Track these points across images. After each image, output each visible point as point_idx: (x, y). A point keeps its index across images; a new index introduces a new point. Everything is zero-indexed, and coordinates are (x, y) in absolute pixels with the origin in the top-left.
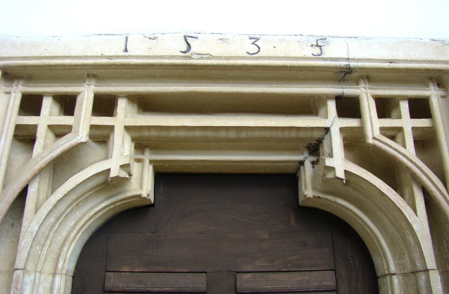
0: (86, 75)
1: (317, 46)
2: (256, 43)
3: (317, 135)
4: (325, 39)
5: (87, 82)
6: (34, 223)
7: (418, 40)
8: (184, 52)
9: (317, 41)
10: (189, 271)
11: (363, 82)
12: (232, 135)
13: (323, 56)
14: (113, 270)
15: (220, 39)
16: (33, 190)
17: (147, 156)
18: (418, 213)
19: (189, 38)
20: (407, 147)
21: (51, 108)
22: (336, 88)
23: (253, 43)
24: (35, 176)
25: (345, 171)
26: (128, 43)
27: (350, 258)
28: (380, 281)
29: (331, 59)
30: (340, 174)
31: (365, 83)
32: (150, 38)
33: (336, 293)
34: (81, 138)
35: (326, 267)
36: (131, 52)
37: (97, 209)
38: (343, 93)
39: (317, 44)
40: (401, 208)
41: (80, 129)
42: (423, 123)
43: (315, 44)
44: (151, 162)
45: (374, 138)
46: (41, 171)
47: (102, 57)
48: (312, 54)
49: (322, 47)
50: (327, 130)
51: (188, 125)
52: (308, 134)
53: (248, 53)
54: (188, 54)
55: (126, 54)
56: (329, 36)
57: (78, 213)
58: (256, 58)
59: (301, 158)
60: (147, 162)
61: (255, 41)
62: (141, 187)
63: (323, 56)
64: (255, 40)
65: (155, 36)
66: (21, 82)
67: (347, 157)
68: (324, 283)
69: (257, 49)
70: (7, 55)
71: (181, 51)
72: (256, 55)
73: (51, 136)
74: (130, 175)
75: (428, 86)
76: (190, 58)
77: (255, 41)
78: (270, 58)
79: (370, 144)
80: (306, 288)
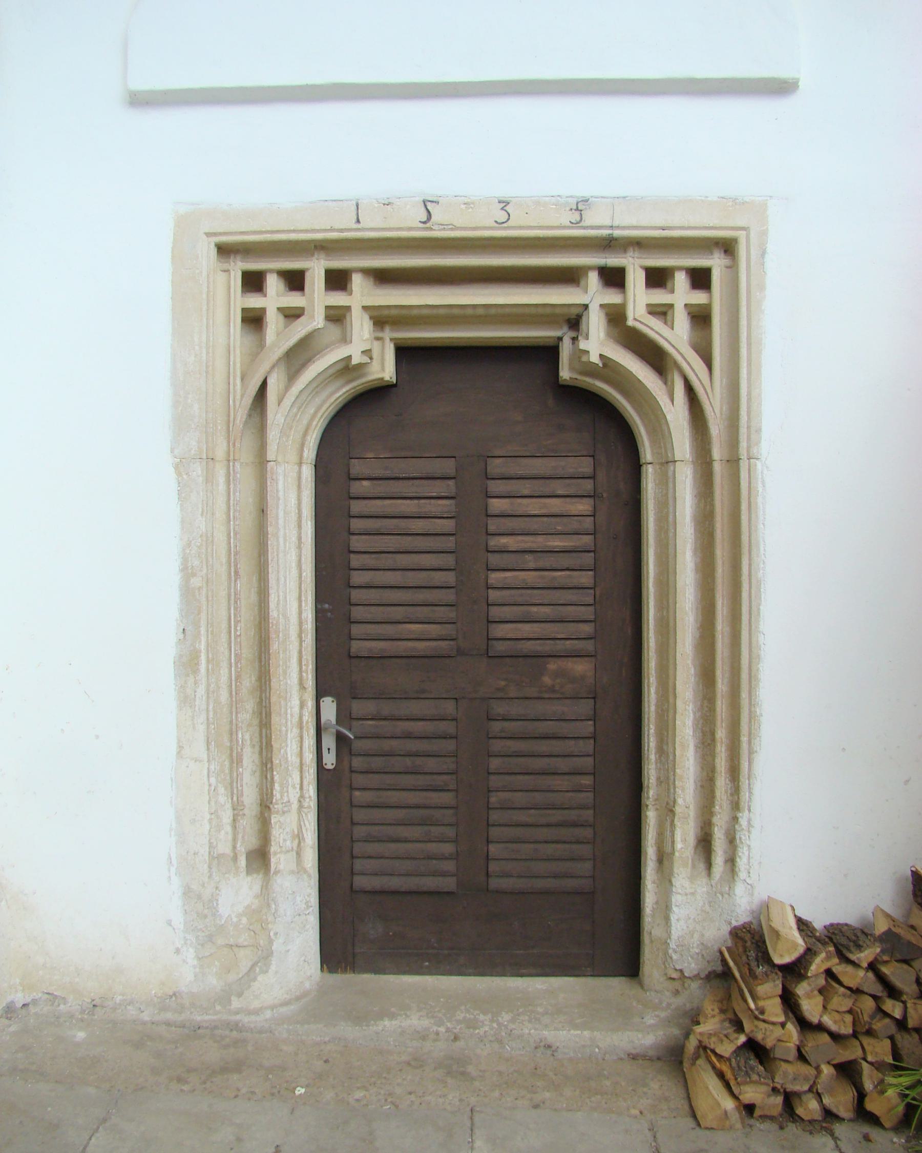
0: (313, 247)
1: (577, 209)
2: (505, 208)
3: (574, 311)
4: (587, 201)
5: (316, 256)
6: (279, 415)
7: (703, 198)
8: (424, 223)
9: (577, 204)
10: (438, 456)
11: (631, 249)
12: (481, 311)
14: (358, 456)
15: (465, 204)
16: (273, 381)
17: (388, 334)
19: (429, 203)
21: (277, 286)
22: (599, 258)
23: (502, 209)
24: (273, 367)
25: (601, 355)
26: (360, 211)
27: (612, 444)
28: (644, 468)
29: (592, 228)
30: (594, 358)
31: (634, 251)
32: (384, 204)
34: (318, 324)
35: (585, 453)
36: (366, 222)
37: (338, 395)
38: (606, 265)
39: (577, 207)
40: (656, 397)
41: (316, 313)
42: (699, 298)
43: (575, 207)
44: (391, 340)
45: (635, 319)
46: (280, 359)
47: (332, 230)
48: (570, 222)
49: (582, 212)
50: (586, 307)
51: (431, 304)
52: (565, 310)
53: (496, 222)
54: (428, 225)
55: (359, 226)
56: (592, 197)
57: (317, 399)
58: (505, 228)
59: (558, 333)
60: (387, 340)
61: (505, 206)
62: (383, 369)
64: (505, 204)
65: (390, 201)
66: (239, 257)
67: (609, 335)
68: (580, 470)
69: (507, 216)
70: (221, 230)
71: (420, 222)
72: (505, 225)
73: (281, 318)
74: (371, 358)
75: (712, 254)
76: (431, 229)
77: (505, 206)
78: (521, 228)
79: (630, 327)
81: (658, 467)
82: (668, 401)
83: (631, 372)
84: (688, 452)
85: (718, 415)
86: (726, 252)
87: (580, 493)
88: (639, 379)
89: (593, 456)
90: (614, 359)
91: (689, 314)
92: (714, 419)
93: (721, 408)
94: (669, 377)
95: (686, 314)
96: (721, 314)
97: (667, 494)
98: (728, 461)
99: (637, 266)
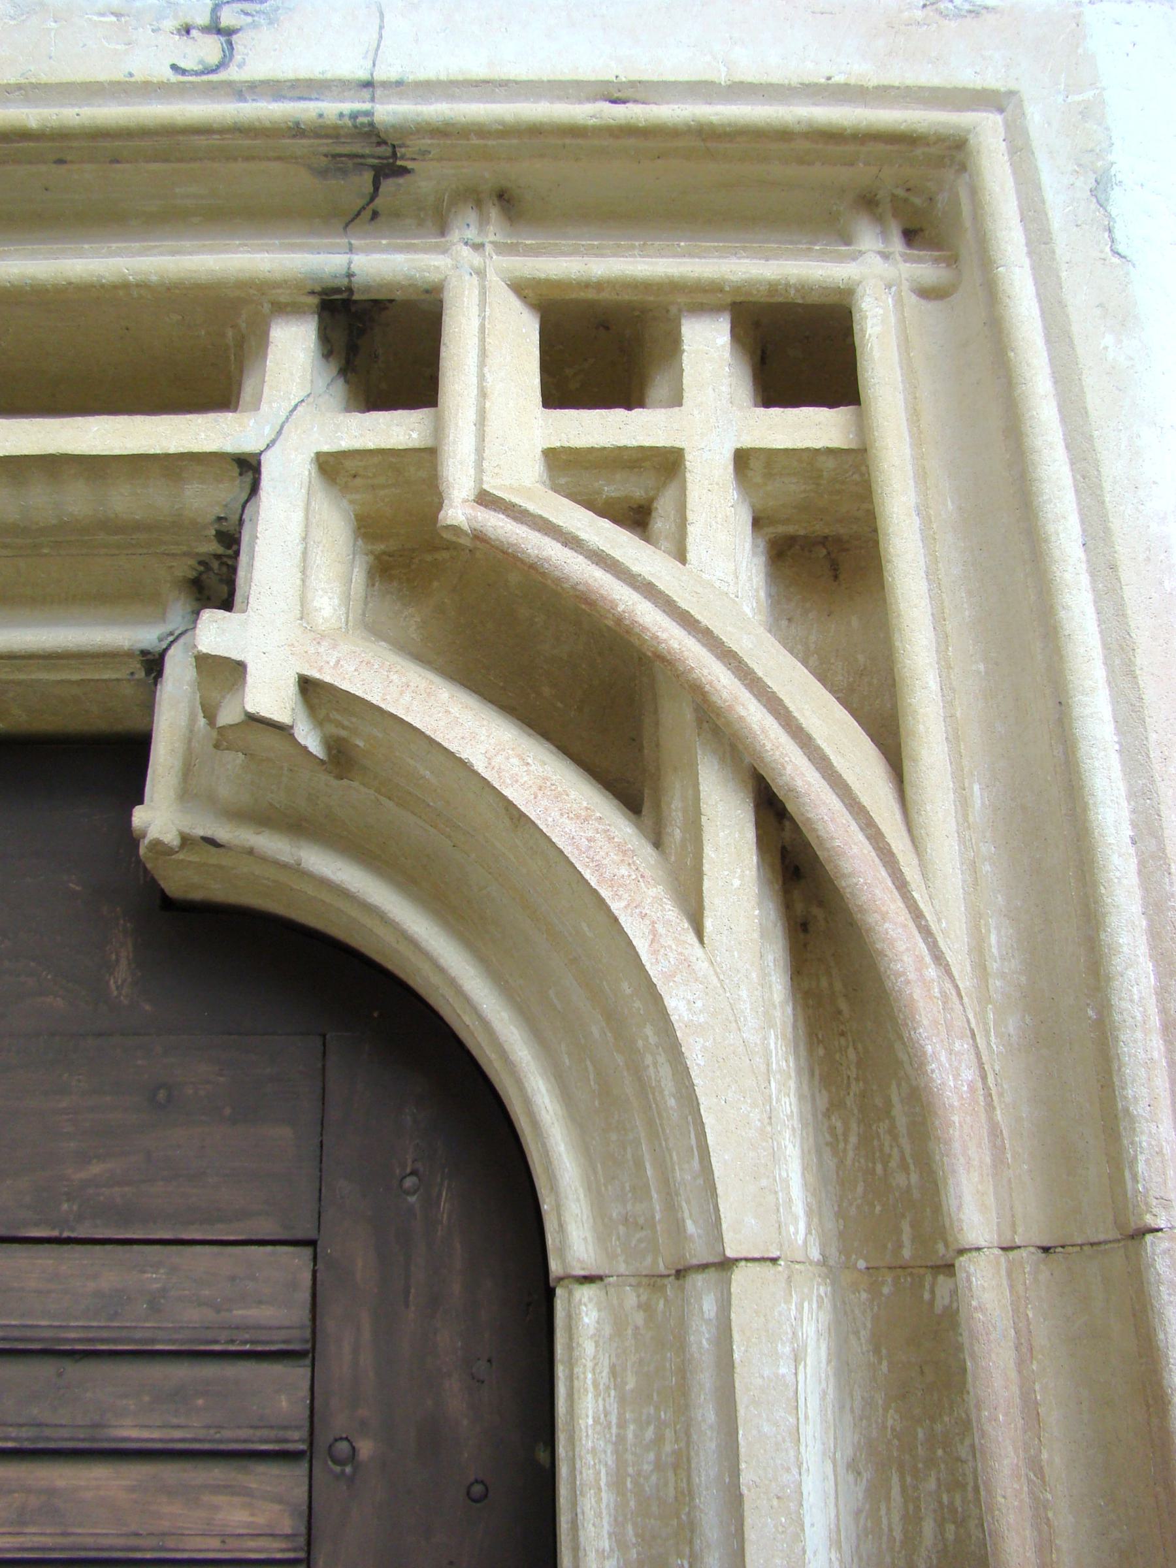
1: (215, 28)
11: (472, 216)
13: (233, 73)
18: (709, 924)
20: (690, 556)
25: (307, 686)
29: (275, 89)
31: (483, 222)
33: (305, 1366)
35: (267, 1228)
38: (350, 275)
40: (604, 893)
43: (203, 19)
45: (485, 499)
48: (174, 67)
49: (234, 38)
59: (146, 636)
63: (233, 73)
75: (847, 240)
80: (138, 1335)
81: (631, 1298)
82: (671, 914)
83: (465, 766)
84: (799, 1208)
85: (965, 984)
86: (911, 236)
87: (232, 1436)
88: (509, 805)
89: (312, 1243)
90: (375, 698)
91: (758, 523)
92: (945, 996)
93: (978, 950)
94: (675, 808)
95: (745, 519)
96: (921, 476)
97: (682, 1463)
98: (1046, 1250)
99: (493, 278)
